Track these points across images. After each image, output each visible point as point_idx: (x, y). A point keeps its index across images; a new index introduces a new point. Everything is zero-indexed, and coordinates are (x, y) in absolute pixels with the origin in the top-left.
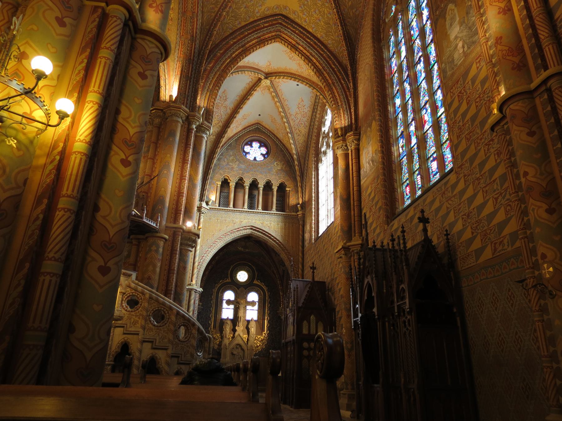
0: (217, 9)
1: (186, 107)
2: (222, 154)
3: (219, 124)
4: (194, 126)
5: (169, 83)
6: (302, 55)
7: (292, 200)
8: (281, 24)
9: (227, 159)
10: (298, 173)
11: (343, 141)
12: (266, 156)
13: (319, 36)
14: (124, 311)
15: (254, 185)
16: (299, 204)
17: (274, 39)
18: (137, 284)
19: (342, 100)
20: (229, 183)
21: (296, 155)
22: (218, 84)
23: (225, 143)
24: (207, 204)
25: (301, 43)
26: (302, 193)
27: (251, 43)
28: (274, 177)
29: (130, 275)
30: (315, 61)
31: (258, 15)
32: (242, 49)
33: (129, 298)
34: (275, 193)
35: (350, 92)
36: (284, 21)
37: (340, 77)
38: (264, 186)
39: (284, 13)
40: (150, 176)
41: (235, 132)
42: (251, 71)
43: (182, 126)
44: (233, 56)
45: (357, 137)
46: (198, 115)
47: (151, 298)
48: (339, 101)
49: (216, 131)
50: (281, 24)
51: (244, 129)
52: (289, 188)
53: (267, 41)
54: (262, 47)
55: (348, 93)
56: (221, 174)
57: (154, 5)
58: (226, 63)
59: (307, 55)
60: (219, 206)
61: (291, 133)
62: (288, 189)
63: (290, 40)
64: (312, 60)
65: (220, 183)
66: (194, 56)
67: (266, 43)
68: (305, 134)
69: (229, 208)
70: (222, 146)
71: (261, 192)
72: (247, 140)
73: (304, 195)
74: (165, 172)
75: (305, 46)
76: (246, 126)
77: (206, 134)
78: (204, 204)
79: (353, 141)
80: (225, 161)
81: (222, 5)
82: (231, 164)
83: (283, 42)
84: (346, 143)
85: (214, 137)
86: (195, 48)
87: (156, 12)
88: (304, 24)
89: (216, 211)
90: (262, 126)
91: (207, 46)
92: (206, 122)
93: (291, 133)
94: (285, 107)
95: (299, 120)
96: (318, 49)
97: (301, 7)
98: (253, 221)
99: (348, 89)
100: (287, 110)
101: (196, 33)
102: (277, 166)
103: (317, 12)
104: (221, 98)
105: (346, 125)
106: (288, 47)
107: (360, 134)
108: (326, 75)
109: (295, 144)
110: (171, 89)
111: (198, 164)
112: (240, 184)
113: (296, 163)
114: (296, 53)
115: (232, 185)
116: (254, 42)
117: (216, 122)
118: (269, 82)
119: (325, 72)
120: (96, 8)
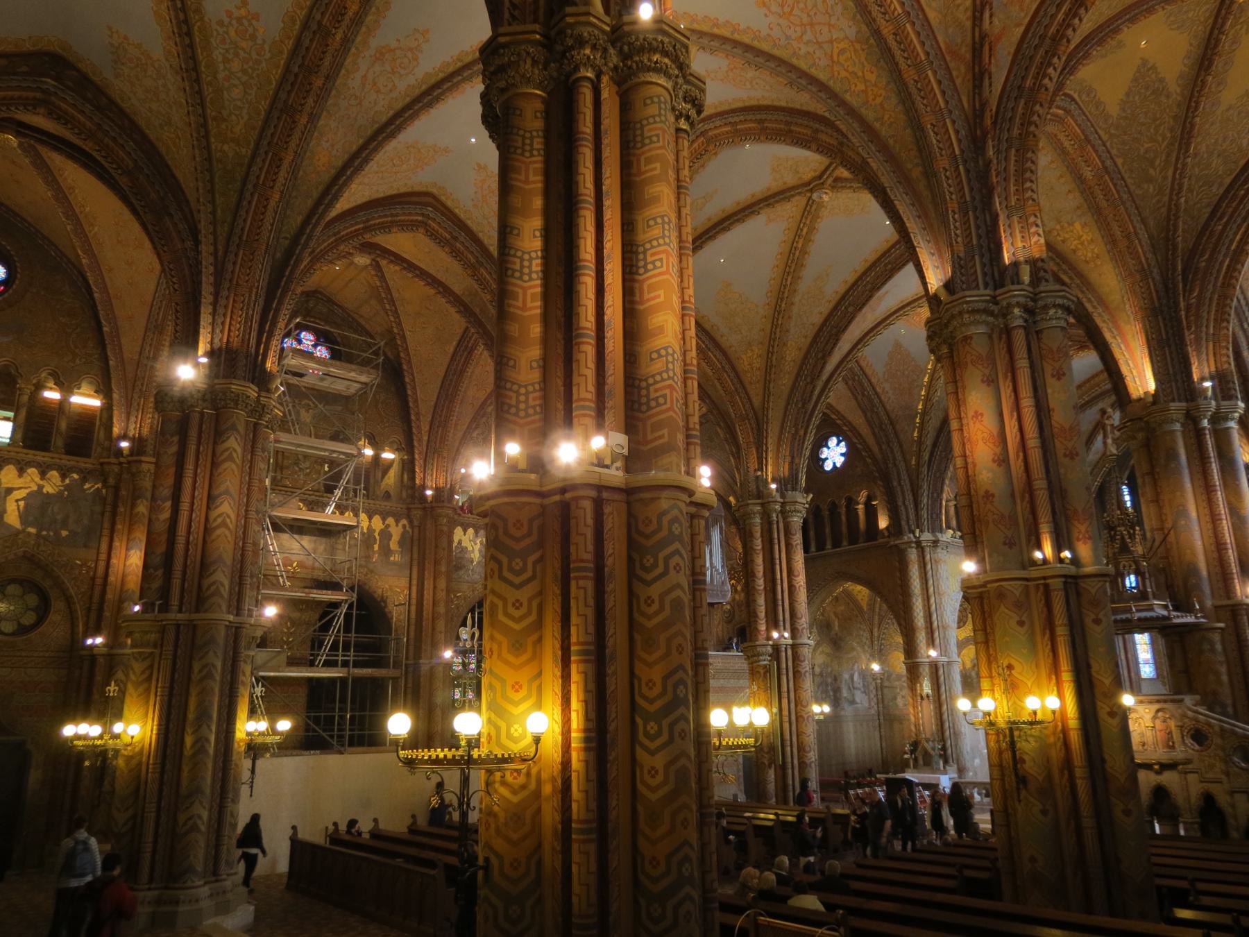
0: (1166, 199)
1: (1180, 401)
4: (1205, 423)
5: (1136, 366)
14: (1191, 751)
18: (1197, 712)
29: (1181, 701)
33: (1192, 732)
40: (1162, 529)
43: (1183, 432)
44: (1233, 247)
47: (1222, 729)
58: (1224, 268)
66: (1159, 299)
77: (1232, 419)
81: (1172, 189)
86: (1155, 285)
87: (1085, 543)
91: (1174, 269)
101: (1147, 259)
110: (1142, 375)
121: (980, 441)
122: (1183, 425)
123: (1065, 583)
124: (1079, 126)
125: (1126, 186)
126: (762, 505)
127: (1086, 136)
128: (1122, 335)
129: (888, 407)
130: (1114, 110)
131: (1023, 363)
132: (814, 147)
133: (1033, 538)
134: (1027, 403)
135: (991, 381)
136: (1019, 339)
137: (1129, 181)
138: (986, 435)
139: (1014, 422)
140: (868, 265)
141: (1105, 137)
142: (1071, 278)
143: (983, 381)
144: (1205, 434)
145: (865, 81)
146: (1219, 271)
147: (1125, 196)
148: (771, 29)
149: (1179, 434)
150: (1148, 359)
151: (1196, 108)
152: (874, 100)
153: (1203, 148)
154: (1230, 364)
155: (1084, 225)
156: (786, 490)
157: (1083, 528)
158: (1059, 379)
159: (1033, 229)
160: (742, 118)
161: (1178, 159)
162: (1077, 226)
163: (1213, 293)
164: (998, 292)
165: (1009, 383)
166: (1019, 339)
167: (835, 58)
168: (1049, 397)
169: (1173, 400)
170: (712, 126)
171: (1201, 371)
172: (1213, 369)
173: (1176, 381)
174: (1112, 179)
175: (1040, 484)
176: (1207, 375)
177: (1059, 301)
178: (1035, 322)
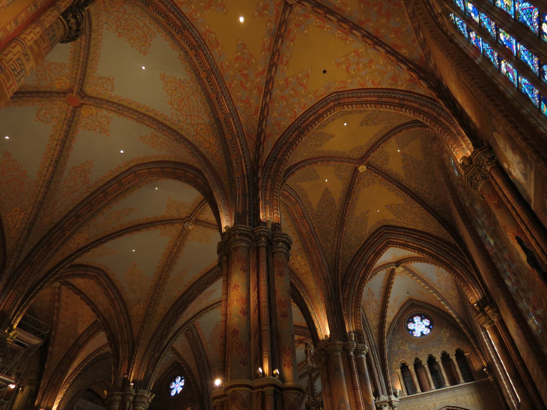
0: (335, 250)
1: (340, 341)
2: (390, 340)
3: (377, 317)
4: (352, 353)
5: (322, 324)
6: (415, 249)
7: (476, 365)
8: (386, 233)
9: (397, 344)
10: (468, 335)
11: (484, 316)
12: (431, 327)
13: (421, 229)
15: (431, 361)
16: (484, 367)
17: (386, 246)
19: (466, 275)
20: (408, 366)
21: (458, 318)
22: (358, 304)
23: (389, 330)
24: (396, 396)
25: (410, 241)
26: (482, 354)
27: (370, 259)
28: (447, 346)
30: (427, 250)
31: (366, 236)
32: (365, 267)
34: (455, 362)
35: (469, 266)
36: (388, 230)
37: (455, 256)
38: (442, 358)
39: (385, 224)
41: (393, 315)
42: (382, 269)
43: (342, 357)
44: (361, 276)
45: (496, 309)
46: (351, 342)
48: (464, 277)
49: (377, 324)
50: (386, 233)
51: (400, 309)
52: (467, 352)
53: (382, 251)
54: (380, 258)
55: (468, 267)
56: (397, 360)
57: (286, 364)
59: (418, 248)
60: (408, 394)
61: (443, 299)
62: (466, 354)
63: (400, 241)
64: (424, 250)
65: (400, 370)
66: (331, 293)
67: (382, 252)
68: (457, 295)
69: (417, 394)
70: (388, 333)
71: (441, 366)
72: (407, 319)
73: (485, 356)
74: (343, 406)
75: (413, 241)
76: (400, 306)
77: (364, 354)
78: (393, 398)
79: (494, 315)
80: (395, 347)
82: (402, 347)
83: (395, 245)
84: (489, 317)
85: (377, 329)
86: (330, 287)
87: (289, 368)
88: (404, 225)
89: (407, 401)
90: (415, 300)
91: (338, 281)
92: (359, 344)
93: (443, 301)
94: (425, 280)
95: (444, 286)
96: (425, 239)
97: (395, 215)
98: (447, 400)
99: (467, 263)
100: (428, 282)
101: (327, 275)
102: (445, 334)
103: (410, 214)
104: (368, 295)
105: (481, 298)
106: (400, 248)
107: (496, 305)
108: (442, 258)
109: (451, 308)
111: (366, 385)
112: (418, 364)
113: (461, 326)
114: (408, 250)
115: (411, 368)
116: (372, 257)
117: (374, 316)
118: (401, 268)
119: (440, 257)
120: (258, 392)
121: (235, 301)
122: (342, 353)
123: (275, 392)
124: (301, 209)
125: (319, 241)
126: (123, 396)
127: (304, 215)
128: (316, 309)
129: (209, 358)
130: (315, 207)
131: (263, 264)
132: (184, 179)
133: (258, 361)
134: (263, 283)
135: (246, 271)
136: (263, 252)
137: (320, 240)
138: (238, 297)
139: (256, 293)
140: (207, 271)
141: (311, 218)
142: (295, 281)
143: (241, 269)
144: (352, 359)
145: (210, 143)
146: (355, 285)
147: (319, 246)
148: (173, 116)
149: (340, 358)
150: (327, 320)
151: (346, 213)
152: (212, 151)
153: (349, 232)
154: (361, 327)
155: (302, 257)
156: (140, 388)
157: (288, 358)
158: (281, 276)
159: (275, 211)
160: (154, 166)
161: (339, 234)
162: (299, 257)
163: (353, 294)
164: (255, 229)
165: (255, 273)
166: (263, 252)
167: (198, 132)
168: (276, 285)
169: (338, 340)
170: (139, 169)
171: (349, 329)
172: (354, 329)
173: (339, 332)
174: (314, 237)
175: (266, 327)
176: (352, 331)
177: (284, 239)
178: (272, 248)
